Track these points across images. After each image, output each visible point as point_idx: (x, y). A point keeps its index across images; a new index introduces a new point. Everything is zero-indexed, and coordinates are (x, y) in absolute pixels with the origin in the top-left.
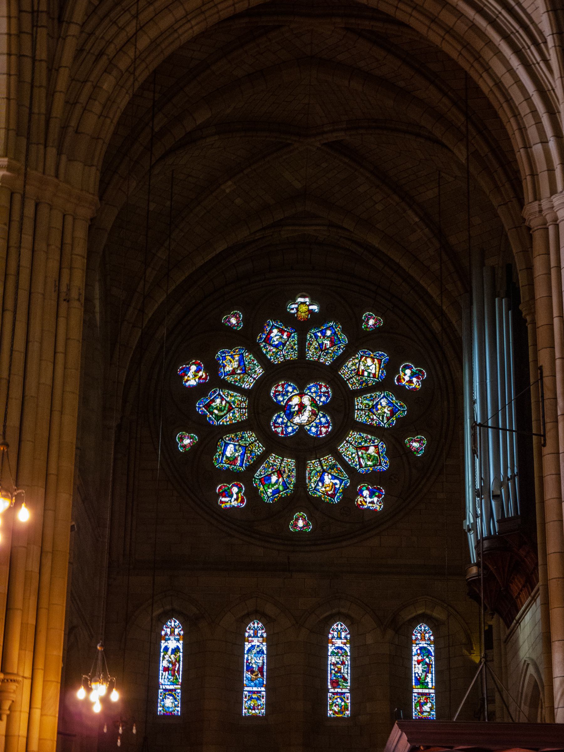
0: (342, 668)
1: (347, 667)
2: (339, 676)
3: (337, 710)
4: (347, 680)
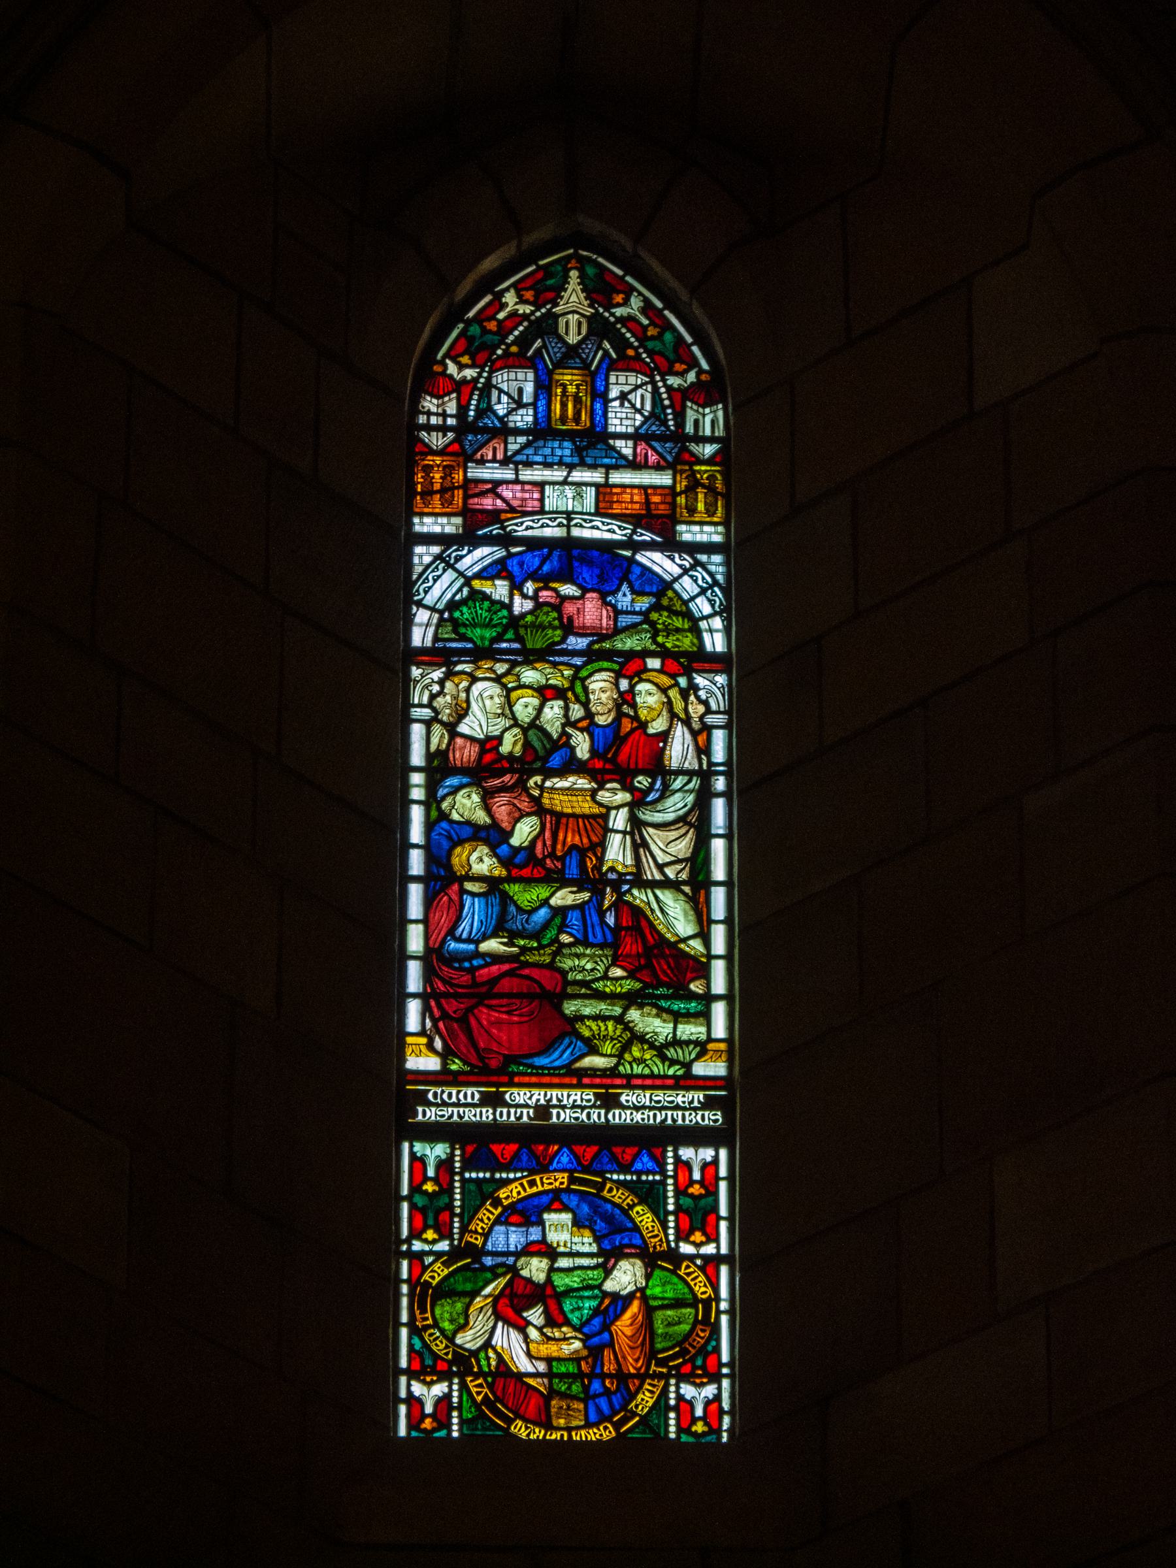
0: (619, 820)
1: (677, 804)
2: (562, 911)
3: (524, 1364)
4: (703, 970)
